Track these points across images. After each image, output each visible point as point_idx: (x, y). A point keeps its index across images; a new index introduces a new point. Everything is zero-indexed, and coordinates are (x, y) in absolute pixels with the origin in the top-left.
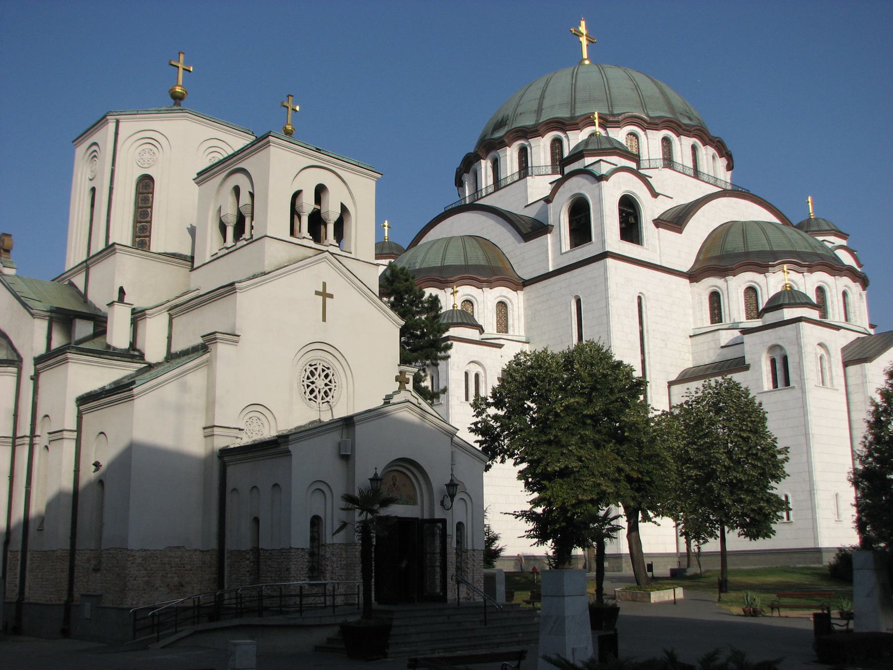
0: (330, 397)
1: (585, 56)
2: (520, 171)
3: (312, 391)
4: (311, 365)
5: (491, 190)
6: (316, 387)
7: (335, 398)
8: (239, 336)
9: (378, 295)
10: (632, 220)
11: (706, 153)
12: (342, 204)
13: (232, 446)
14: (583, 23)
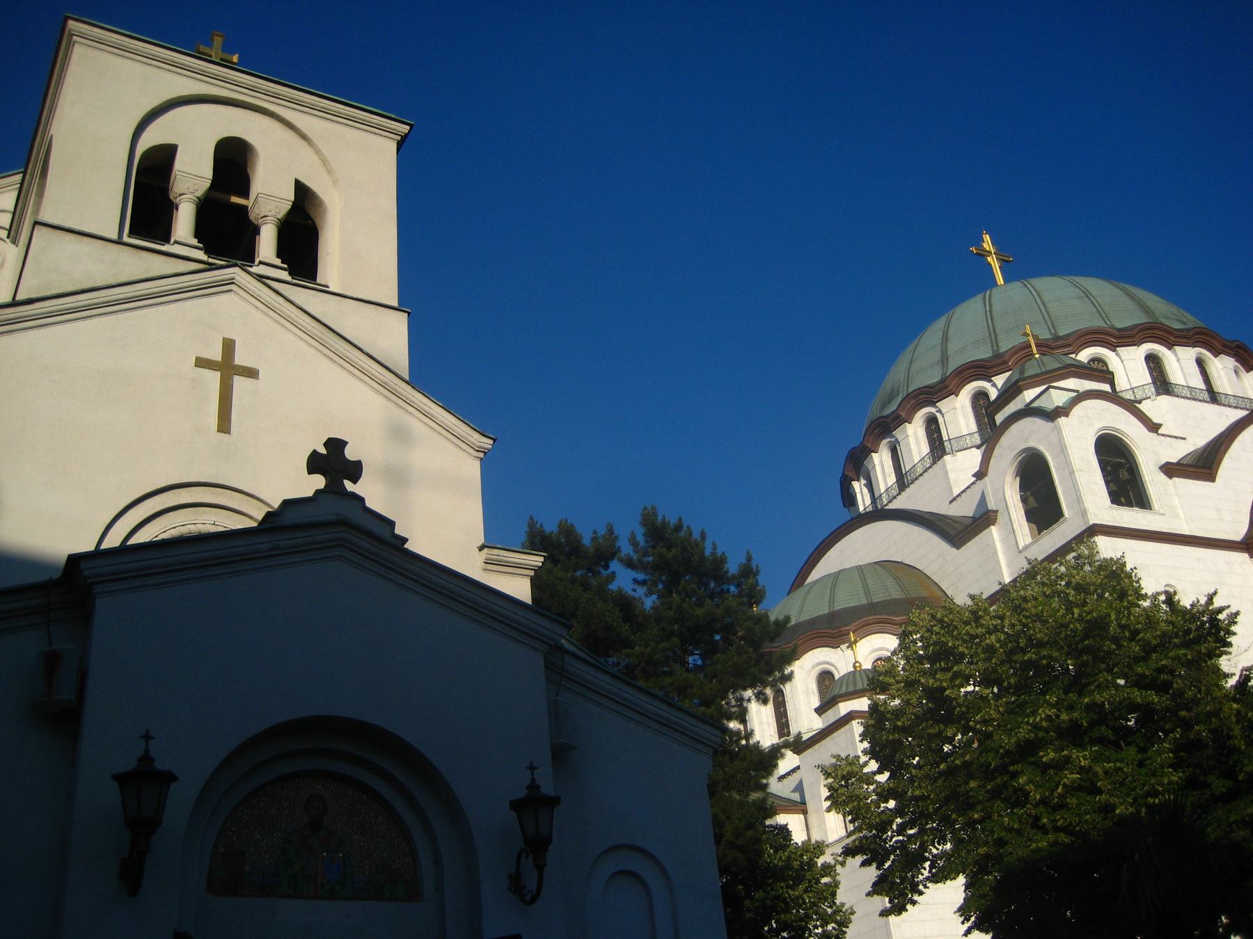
2: (932, 451)
5: (895, 492)
10: (1124, 475)
14: (987, 238)
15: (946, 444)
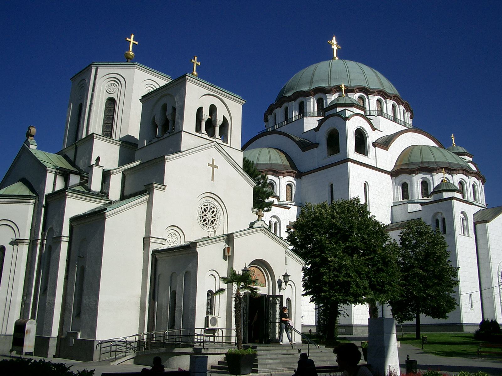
0: (214, 224)
1: (335, 55)
3: (205, 220)
4: (204, 205)
6: (207, 218)
7: (217, 225)
8: (166, 186)
9: (242, 167)
11: (400, 109)
12: (224, 116)
13: (160, 249)
15: (305, 113)
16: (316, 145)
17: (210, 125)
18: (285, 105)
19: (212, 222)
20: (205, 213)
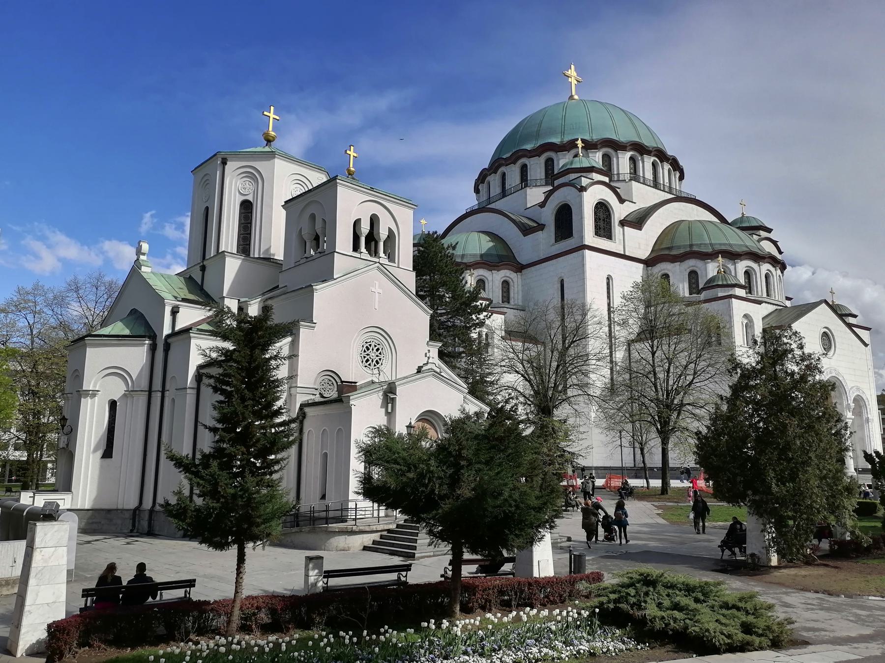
3: (367, 361)
4: (366, 343)
6: (370, 358)
8: (315, 323)
16: (541, 227)
17: (372, 238)
18: (502, 169)
19: (377, 362)
20: (368, 352)
